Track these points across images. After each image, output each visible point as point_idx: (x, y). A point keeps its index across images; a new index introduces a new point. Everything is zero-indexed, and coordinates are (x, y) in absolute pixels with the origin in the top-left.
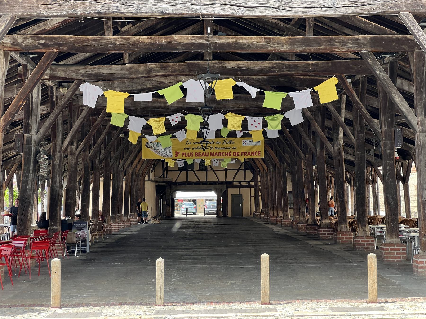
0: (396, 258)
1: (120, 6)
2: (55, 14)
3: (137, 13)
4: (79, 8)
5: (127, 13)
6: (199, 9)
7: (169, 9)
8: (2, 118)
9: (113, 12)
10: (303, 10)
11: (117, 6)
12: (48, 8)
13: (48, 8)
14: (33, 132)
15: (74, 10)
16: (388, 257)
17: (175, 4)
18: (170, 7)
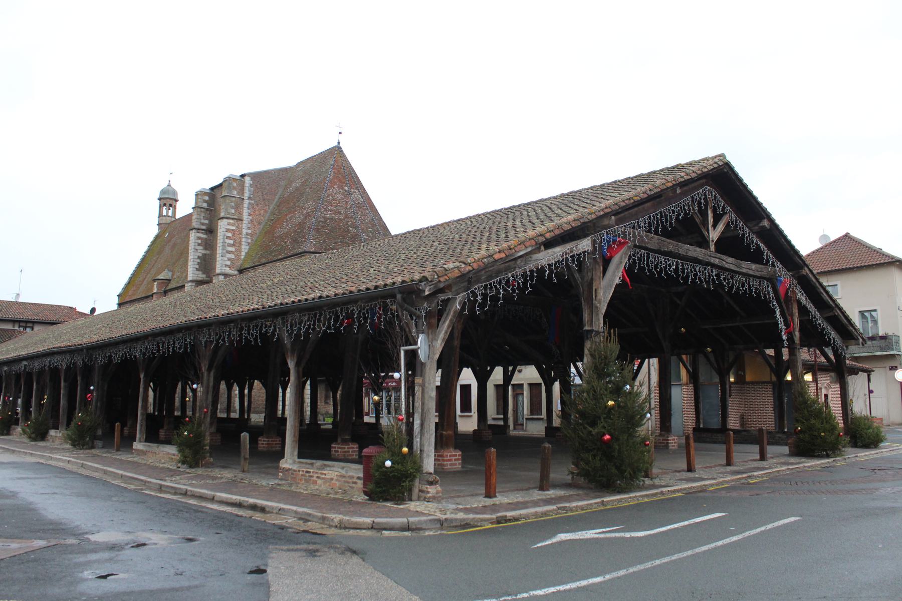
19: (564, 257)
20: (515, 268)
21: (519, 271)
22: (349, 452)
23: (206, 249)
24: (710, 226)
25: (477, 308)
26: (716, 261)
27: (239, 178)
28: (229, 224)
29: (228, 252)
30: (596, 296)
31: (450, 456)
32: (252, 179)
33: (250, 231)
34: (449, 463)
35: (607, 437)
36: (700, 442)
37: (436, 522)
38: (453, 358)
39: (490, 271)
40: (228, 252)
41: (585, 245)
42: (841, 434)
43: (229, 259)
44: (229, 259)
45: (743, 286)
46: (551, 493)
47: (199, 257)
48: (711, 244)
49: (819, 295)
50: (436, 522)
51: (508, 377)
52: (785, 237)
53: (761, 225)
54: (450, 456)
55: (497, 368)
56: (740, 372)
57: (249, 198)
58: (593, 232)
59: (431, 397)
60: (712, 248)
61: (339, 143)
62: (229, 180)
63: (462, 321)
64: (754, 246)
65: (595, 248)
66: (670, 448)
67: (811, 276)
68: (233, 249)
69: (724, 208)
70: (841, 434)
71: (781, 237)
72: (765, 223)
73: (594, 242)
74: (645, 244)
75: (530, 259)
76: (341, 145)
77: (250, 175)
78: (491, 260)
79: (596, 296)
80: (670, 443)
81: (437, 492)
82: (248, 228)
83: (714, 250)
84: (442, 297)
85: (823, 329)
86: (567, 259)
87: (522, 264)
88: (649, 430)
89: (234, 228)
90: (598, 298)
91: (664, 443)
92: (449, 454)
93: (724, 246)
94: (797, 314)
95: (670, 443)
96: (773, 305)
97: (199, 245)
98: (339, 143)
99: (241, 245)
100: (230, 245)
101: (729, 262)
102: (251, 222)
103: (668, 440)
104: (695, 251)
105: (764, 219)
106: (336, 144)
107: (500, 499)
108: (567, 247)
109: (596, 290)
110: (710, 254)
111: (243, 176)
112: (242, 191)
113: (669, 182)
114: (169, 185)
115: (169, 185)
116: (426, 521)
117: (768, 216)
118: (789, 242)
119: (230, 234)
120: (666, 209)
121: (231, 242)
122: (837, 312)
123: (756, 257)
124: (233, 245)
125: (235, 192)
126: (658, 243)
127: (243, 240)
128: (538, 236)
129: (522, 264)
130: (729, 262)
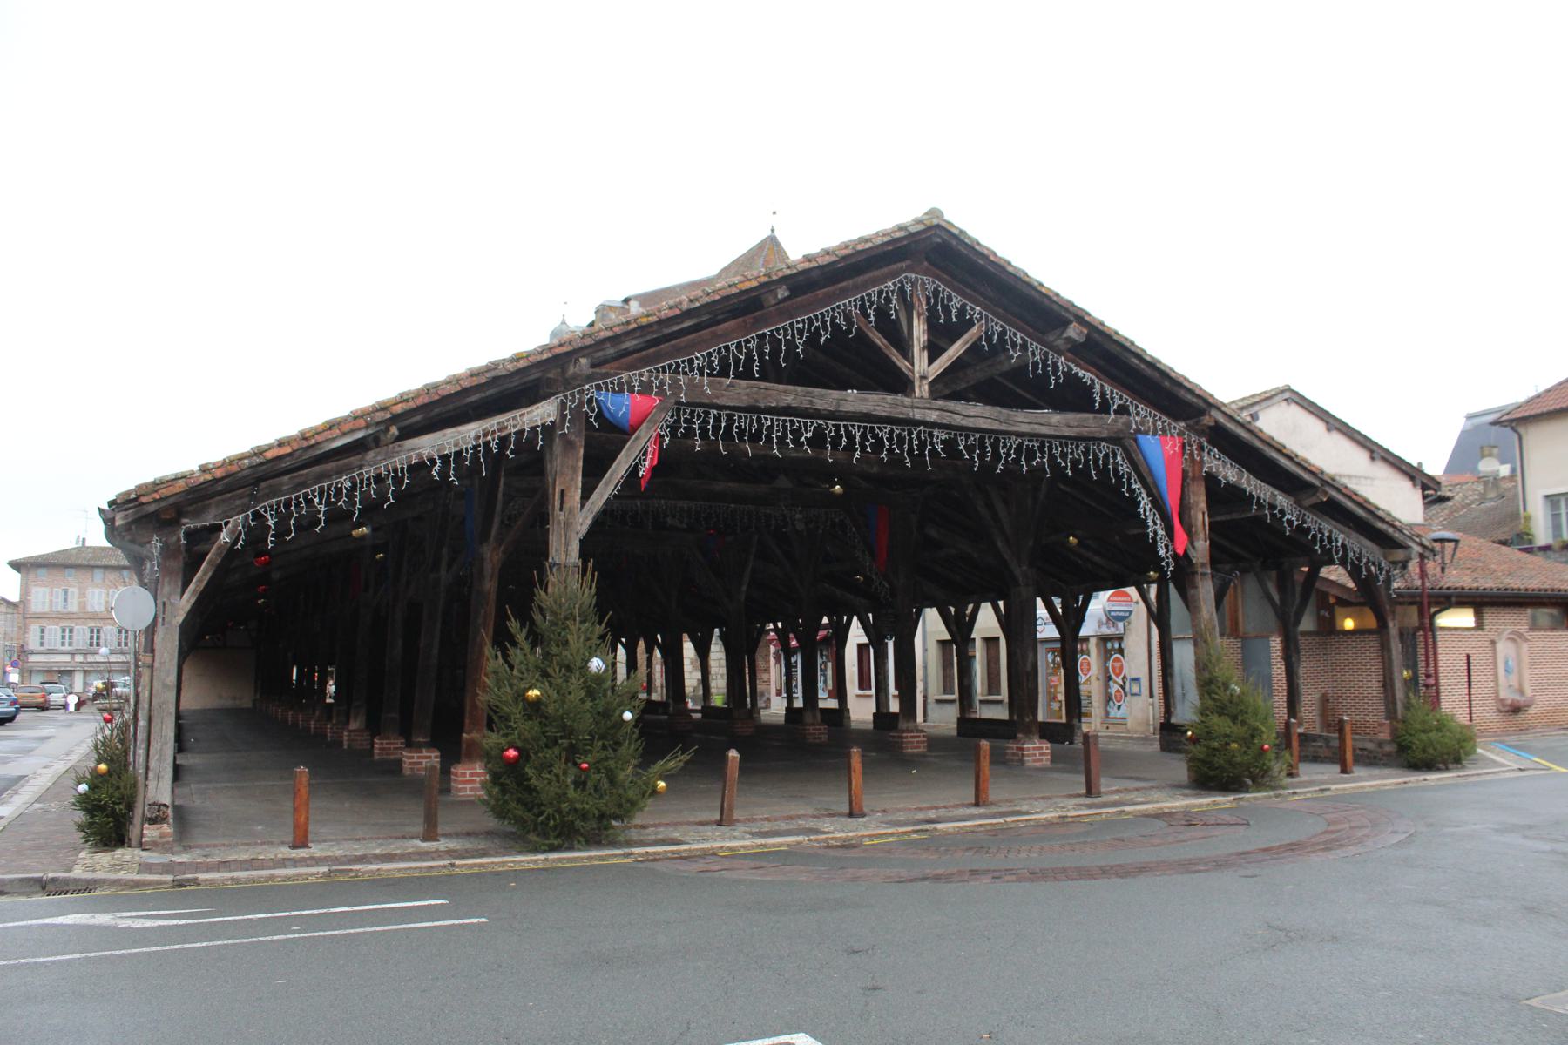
0: (916, 747)
1: (815, 400)
2: (732, 404)
3: (836, 411)
4: (764, 398)
5: (824, 410)
6: (911, 414)
7: (875, 410)
8: (502, 548)
9: (806, 408)
10: (1027, 426)
11: (811, 401)
12: (723, 396)
13: (723, 396)
14: (443, 572)
15: (757, 401)
16: (907, 748)
17: (883, 404)
18: (877, 408)
19: (481, 441)
20: (361, 467)
21: (369, 472)
22: (421, 763)
24: (916, 350)
25: (270, 539)
26: (933, 416)
27: (620, 305)
30: (562, 502)
31: (471, 775)
34: (468, 786)
35: (512, 753)
36: (1170, 751)
37: (32, 883)
38: (483, 611)
39: (302, 475)
41: (543, 412)
42: (1266, 747)
45: (1031, 455)
46: (442, 844)
48: (917, 384)
49: (1273, 464)
50: (32, 883)
51: (1070, 621)
52: (1139, 355)
53: (1065, 336)
54: (471, 775)
55: (983, 605)
56: (1322, 612)
58: (562, 389)
59: (165, 686)
60: (921, 390)
61: (773, 230)
62: (604, 309)
63: (502, 548)
64: (1058, 378)
65: (563, 417)
66: (1027, 764)
67: (1232, 426)
69: (962, 311)
70: (1266, 747)
71: (1126, 354)
72: (1074, 332)
73: (563, 405)
74: (708, 398)
75: (398, 449)
76: (777, 234)
77: (636, 298)
78: (262, 459)
79: (562, 502)
80: (1028, 755)
81: (162, 836)
83: (926, 395)
84: (189, 523)
85: (1302, 530)
86: (487, 444)
87: (379, 458)
88: (1149, 725)
90: (566, 506)
91: (1018, 755)
92: (468, 772)
93: (948, 386)
94: (1203, 505)
95: (1028, 755)
96: (1132, 491)
98: (773, 230)
101: (972, 414)
103: (1022, 749)
104: (866, 400)
105: (1071, 322)
106: (769, 233)
107: (315, 850)
108: (492, 423)
109: (562, 492)
110: (920, 404)
111: (626, 301)
113: (749, 280)
114: (564, 323)
115: (564, 323)
116: (12, 881)
117: (1081, 317)
118: (1153, 365)
120: (778, 330)
122: (1326, 493)
123: (1074, 397)
126: (747, 395)
128: (377, 411)
129: (379, 458)
130: (978, 415)
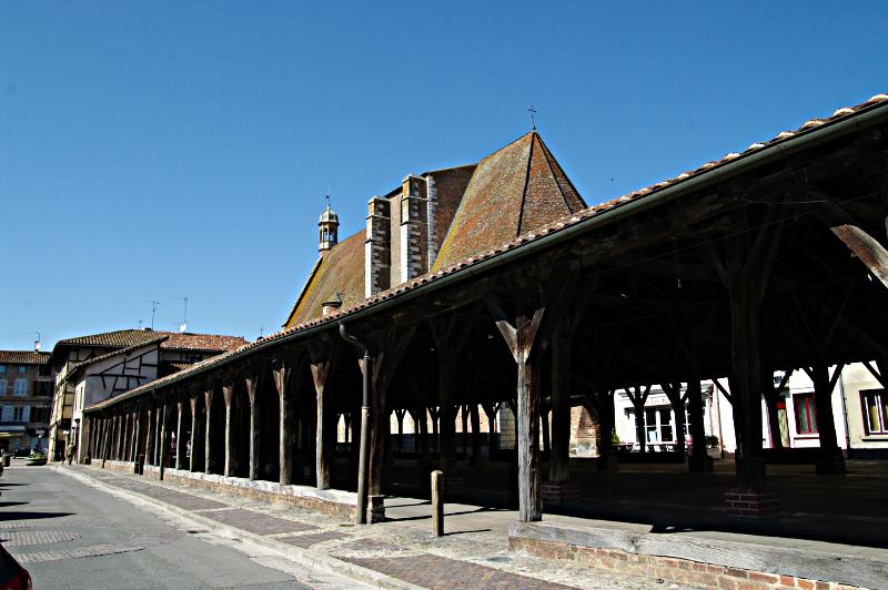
23: (384, 262)
28: (414, 229)
29: (414, 261)
32: (434, 179)
33: (435, 237)
40: (414, 261)
43: (416, 270)
44: (416, 270)
47: (377, 272)
57: (433, 200)
68: (418, 258)
77: (431, 174)
82: (435, 234)
89: (418, 234)
97: (376, 258)
99: (426, 254)
100: (415, 253)
102: (436, 226)
111: (425, 175)
112: (424, 195)
119: (414, 241)
121: (417, 250)
124: (418, 253)
125: (417, 194)
127: (430, 247)
